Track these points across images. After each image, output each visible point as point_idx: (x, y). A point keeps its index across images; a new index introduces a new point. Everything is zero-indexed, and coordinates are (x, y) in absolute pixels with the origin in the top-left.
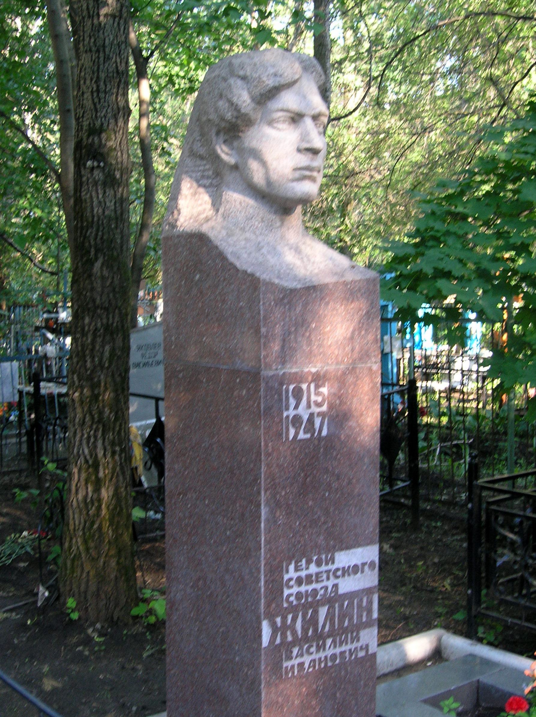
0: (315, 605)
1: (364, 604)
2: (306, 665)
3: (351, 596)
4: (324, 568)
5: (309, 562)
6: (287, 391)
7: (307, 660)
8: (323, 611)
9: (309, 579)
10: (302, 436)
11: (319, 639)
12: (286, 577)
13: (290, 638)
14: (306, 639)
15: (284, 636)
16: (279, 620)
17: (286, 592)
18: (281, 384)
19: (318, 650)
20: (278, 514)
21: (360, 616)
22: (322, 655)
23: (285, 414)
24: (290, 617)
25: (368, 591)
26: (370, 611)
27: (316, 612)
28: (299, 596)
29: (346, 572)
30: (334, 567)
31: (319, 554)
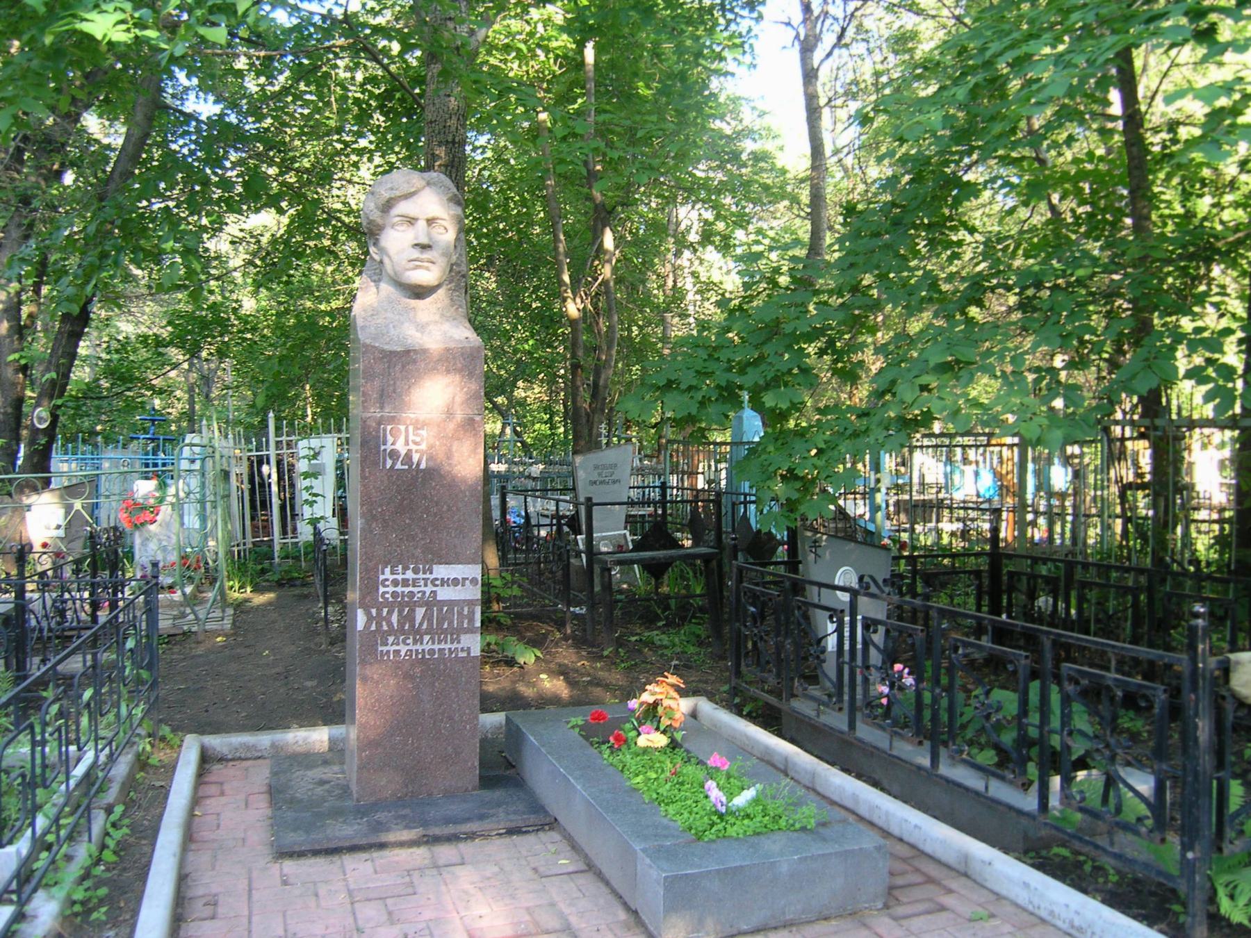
0: (413, 606)
1: (466, 612)
2: (403, 653)
3: (451, 603)
4: (421, 576)
5: (405, 569)
6: (385, 430)
7: (403, 649)
8: (420, 612)
9: (405, 583)
10: (399, 466)
11: (417, 634)
12: (382, 577)
13: (385, 628)
14: (401, 630)
15: (379, 625)
16: (374, 611)
17: (382, 590)
18: (379, 424)
19: (415, 642)
20: (374, 525)
21: (461, 622)
22: (419, 647)
23: (383, 448)
24: (385, 610)
25: (471, 603)
26: (471, 620)
27: (412, 611)
28: (395, 594)
29: (444, 582)
30: (432, 577)
31: (416, 563)
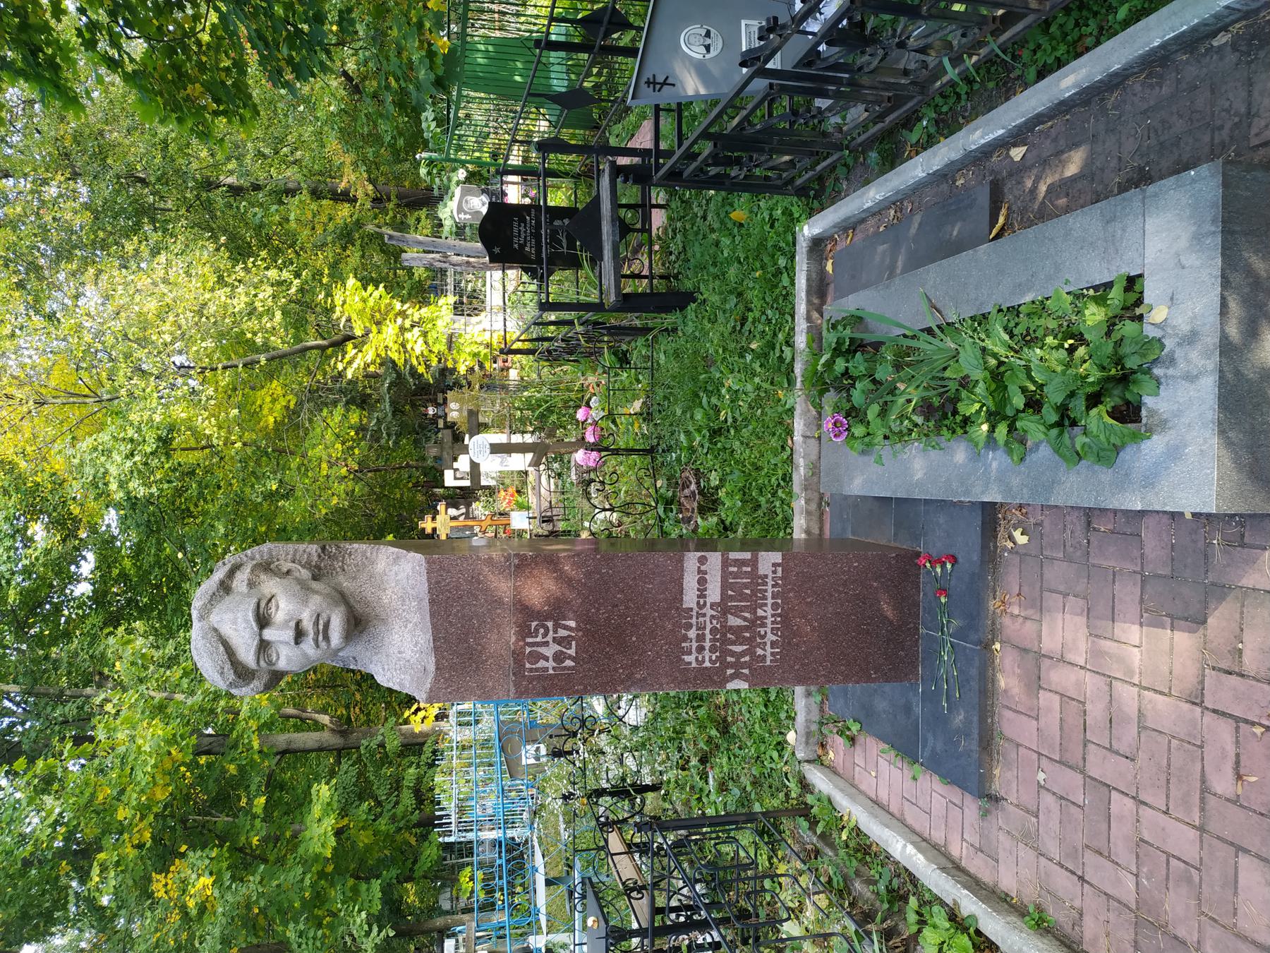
0: (726, 629)
1: (735, 569)
2: (774, 638)
3: (725, 586)
5: (685, 638)
6: (531, 670)
7: (771, 637)
9: (701, 638)
10: (572, 652)
12: (694, 665)
13: (747, 658)
15: (744, 665)
16: (730, 672)
17: (707, 664)
23: (551, 672)
24: (729, 659)
25: (726, 563)
26: (742, 563)
29: (702, 594)
